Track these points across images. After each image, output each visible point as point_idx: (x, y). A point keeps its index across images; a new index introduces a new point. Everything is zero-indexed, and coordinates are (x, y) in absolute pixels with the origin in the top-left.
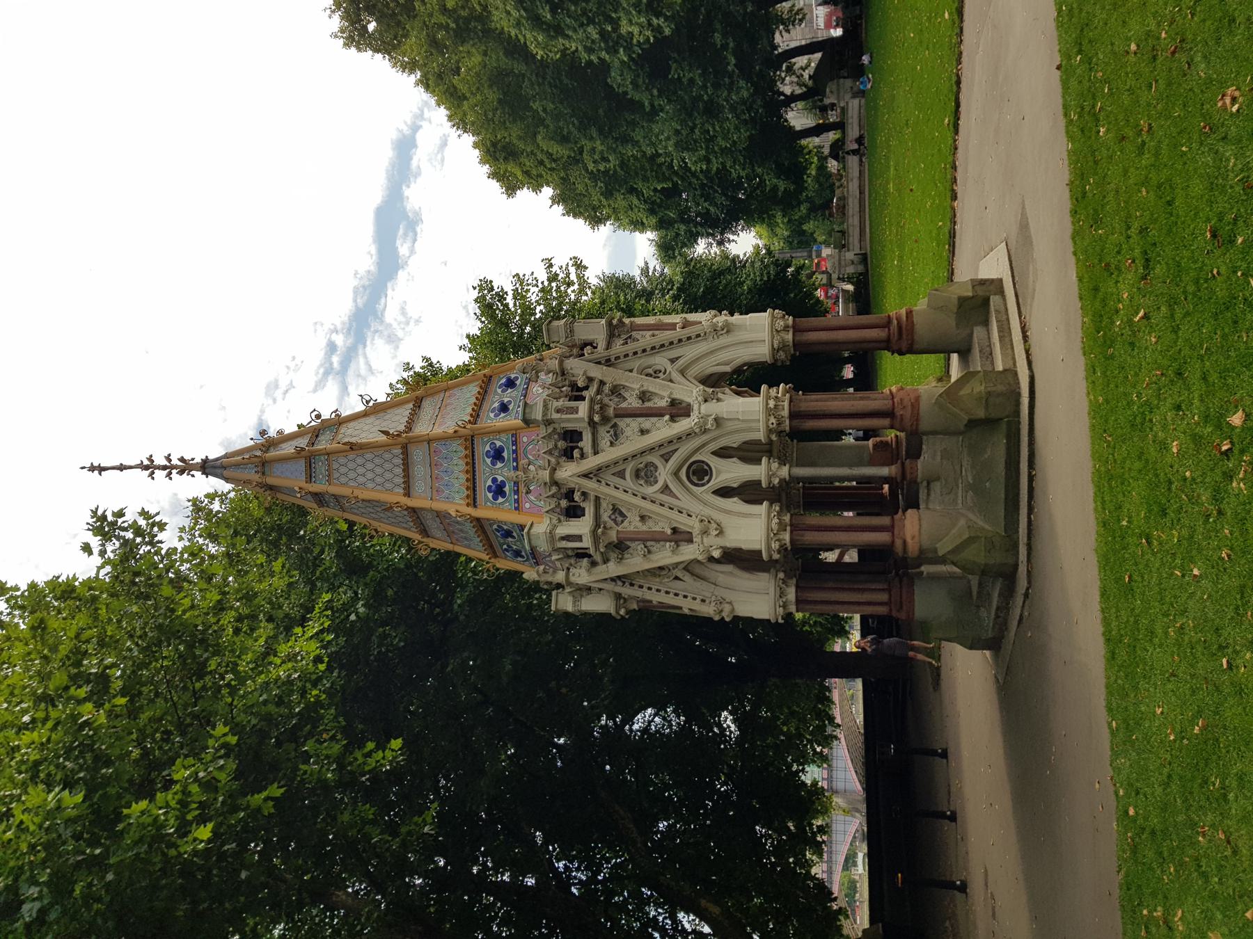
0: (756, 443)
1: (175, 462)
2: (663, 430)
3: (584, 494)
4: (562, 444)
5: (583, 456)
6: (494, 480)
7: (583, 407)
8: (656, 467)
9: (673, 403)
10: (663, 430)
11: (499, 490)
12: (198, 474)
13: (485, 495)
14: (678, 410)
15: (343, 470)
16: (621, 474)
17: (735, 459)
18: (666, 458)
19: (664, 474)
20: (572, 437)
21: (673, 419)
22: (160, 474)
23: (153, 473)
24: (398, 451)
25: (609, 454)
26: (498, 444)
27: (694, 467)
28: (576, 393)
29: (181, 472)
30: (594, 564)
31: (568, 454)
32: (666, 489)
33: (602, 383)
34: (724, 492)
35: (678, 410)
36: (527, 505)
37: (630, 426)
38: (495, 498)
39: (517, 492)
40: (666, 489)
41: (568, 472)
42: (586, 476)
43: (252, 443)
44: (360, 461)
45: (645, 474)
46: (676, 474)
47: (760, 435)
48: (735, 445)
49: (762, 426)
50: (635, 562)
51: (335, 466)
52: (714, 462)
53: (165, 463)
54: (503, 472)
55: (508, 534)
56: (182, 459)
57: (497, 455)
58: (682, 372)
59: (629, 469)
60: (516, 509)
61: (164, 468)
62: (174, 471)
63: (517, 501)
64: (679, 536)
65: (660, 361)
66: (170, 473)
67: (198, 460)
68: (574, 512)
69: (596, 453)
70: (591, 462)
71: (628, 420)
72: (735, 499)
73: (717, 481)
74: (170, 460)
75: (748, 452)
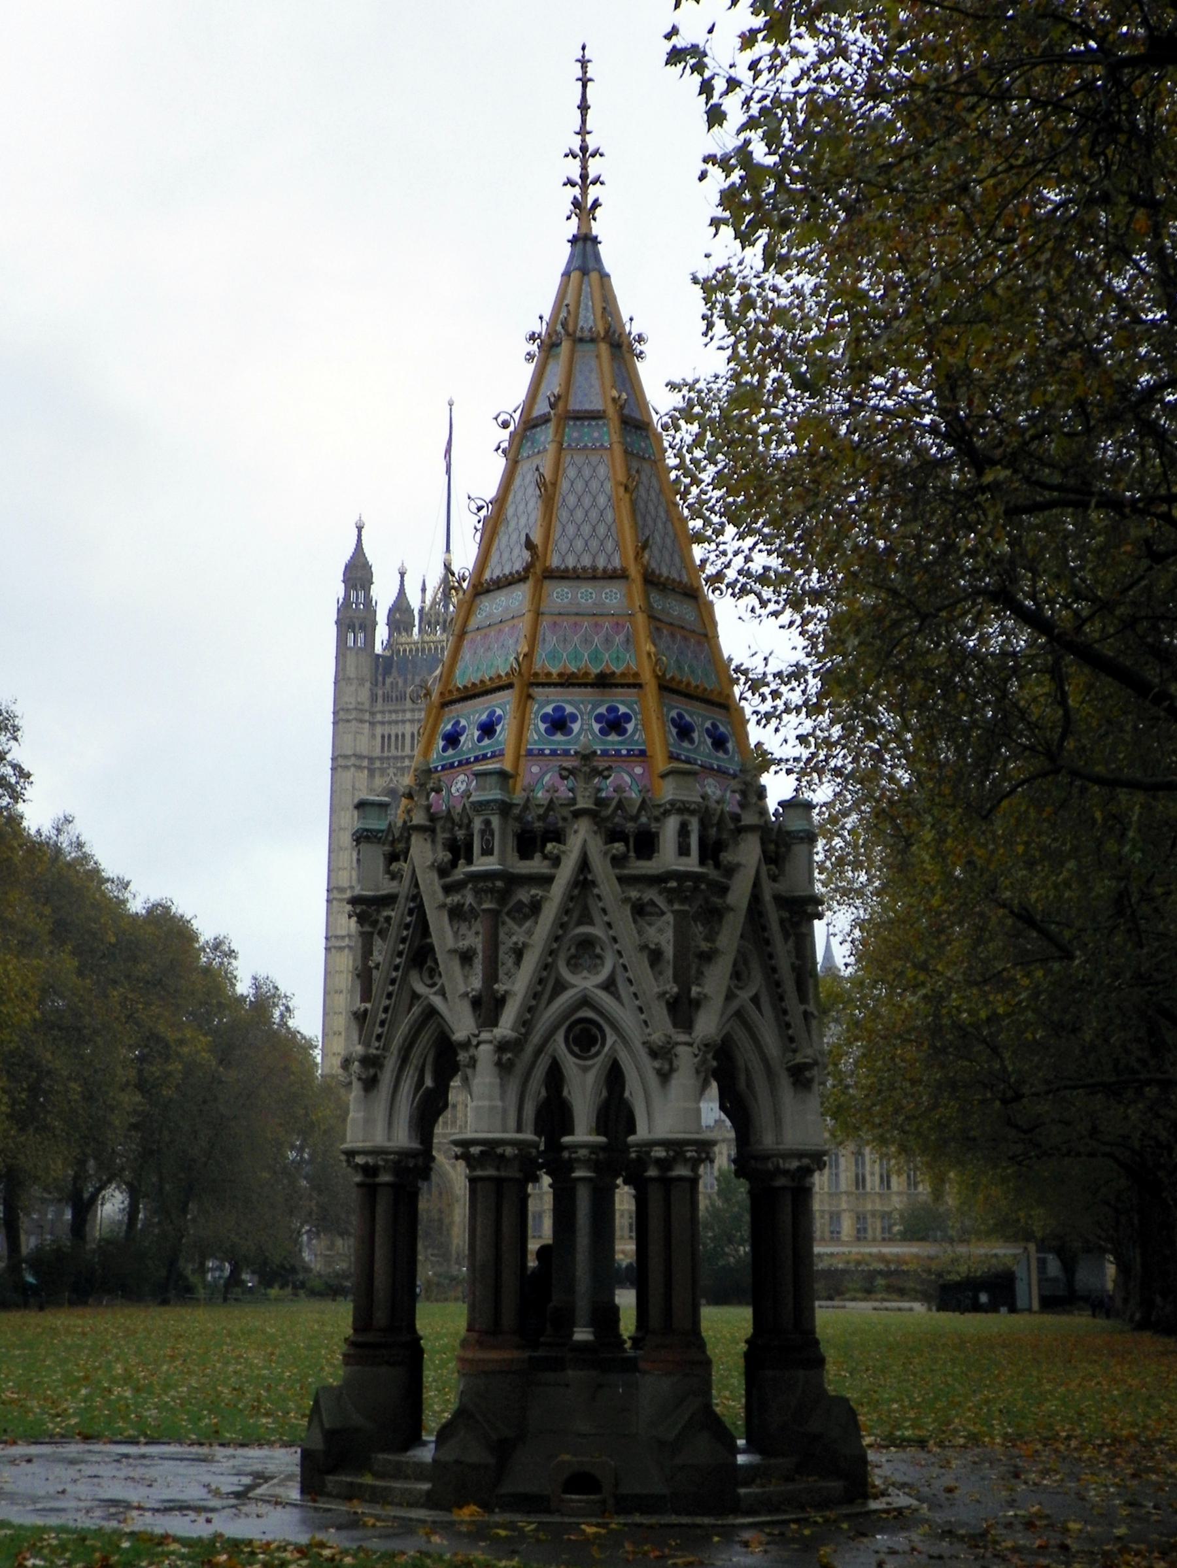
0: (632, 1130)
1: (594, 192)
3: (556, 861)
5: (617, 861)
6: (574, 718)
7: (691, 864)
8: (594, 969)
9: (696, 1004)
11: (559, 723)
12: (572, 227)
13: (547, 701)
14: (682, 1009)
15: (587, 472)
17: (605, 1094)
19: (585, 982)
20: (646, 844)
22: (573, 169)
23: (575, 157)
24: (617, 562)
26: (630, 727)
27: (595, 1031)
28: (711, 851)
29: (576, 203)
30: (443, 872)
31: (613, 836)
32: (560, 986)
33: (724, 890)
34: (555, 1077)
35: (682, 1009)
36: (535, 769)
38: (545, 718)
39: (554, 753)
40: (560, 986)
42: (584, 865)
43: (625, 318)
44: (602, 500)
46: (585, 1001)
47: (642, 1132)
48: (627, 1094)
50: (444, 936)
51: (594, 459)
52: (599, 1063)
53: (591, 177)
54: (585, 732)
55: (488, 729)
56: (596, 204)
57: (614, 724)
58: (739, 1014)
60: (530, 753)
61: (584, 177)
62: (577, 191)
63: (541, 752)
64: (487, 1006)
65: (756, 983)
66: (573, 185)
67: (596, 229)
68: (527, 844)
69: (620, 879)
71: (670, 934)
72: (544, 1093)
73: (570, 1064)
74: (594, 183)
75: (615, 1114)
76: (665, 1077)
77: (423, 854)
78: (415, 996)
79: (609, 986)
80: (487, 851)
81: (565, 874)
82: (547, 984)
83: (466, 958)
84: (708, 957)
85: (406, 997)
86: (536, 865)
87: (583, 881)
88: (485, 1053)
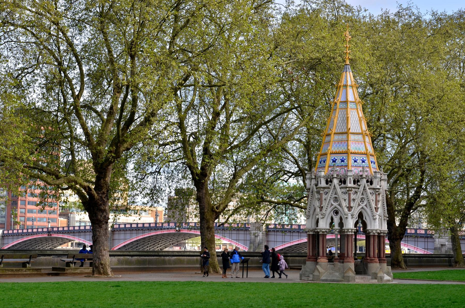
2: (373, 206)
3: (360, 186)
4: (370, 180)
10: (373, 206)
11: (355, 161)
16: (363, 194)
18: (366, 205)
20: (371, 183)
21: (375, 208)
25: (369, 191)
30: (340, 185)
31: (367, 181)
37: (373, 197)
38: (353, 160)
40: (359, 205)
41: (365, 180)
45: (362, 200)
47: (369, 228)
49: (372, 228)
57: (363, 162)
59: (364, 196)
64: (350, 208)
70: (367, 188)
76: (374, 219)
77: (336, 181)
78: (332, 205)
79: (366, 205)
80: (350, 183)
81: (361, 188)
82: (359, 205)
83: (345, 200)
84: (379, 201)
85: (330, 205)
86: (355, 186)
87: (364, 189)
88: (350, 216)
